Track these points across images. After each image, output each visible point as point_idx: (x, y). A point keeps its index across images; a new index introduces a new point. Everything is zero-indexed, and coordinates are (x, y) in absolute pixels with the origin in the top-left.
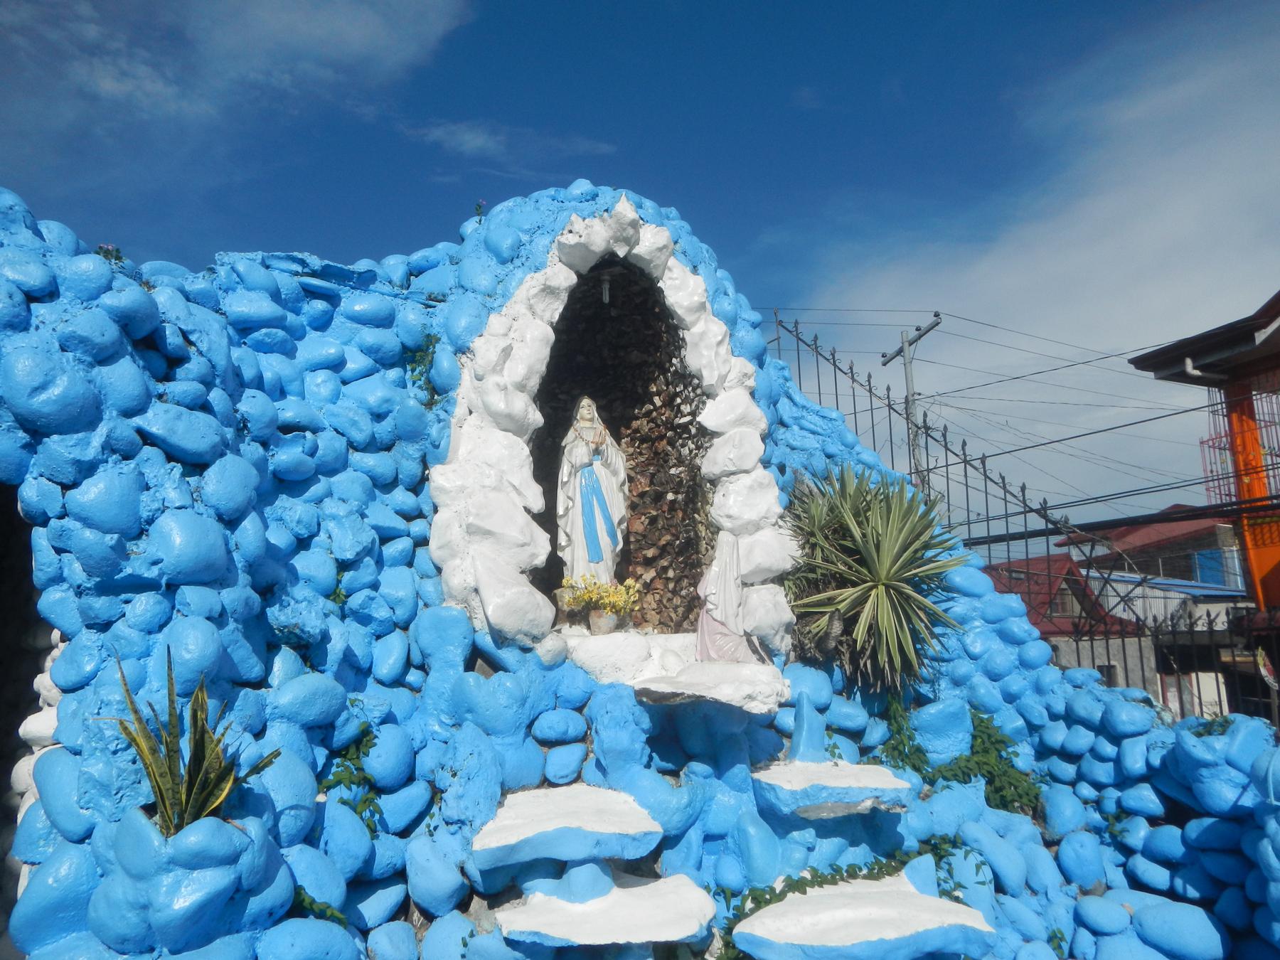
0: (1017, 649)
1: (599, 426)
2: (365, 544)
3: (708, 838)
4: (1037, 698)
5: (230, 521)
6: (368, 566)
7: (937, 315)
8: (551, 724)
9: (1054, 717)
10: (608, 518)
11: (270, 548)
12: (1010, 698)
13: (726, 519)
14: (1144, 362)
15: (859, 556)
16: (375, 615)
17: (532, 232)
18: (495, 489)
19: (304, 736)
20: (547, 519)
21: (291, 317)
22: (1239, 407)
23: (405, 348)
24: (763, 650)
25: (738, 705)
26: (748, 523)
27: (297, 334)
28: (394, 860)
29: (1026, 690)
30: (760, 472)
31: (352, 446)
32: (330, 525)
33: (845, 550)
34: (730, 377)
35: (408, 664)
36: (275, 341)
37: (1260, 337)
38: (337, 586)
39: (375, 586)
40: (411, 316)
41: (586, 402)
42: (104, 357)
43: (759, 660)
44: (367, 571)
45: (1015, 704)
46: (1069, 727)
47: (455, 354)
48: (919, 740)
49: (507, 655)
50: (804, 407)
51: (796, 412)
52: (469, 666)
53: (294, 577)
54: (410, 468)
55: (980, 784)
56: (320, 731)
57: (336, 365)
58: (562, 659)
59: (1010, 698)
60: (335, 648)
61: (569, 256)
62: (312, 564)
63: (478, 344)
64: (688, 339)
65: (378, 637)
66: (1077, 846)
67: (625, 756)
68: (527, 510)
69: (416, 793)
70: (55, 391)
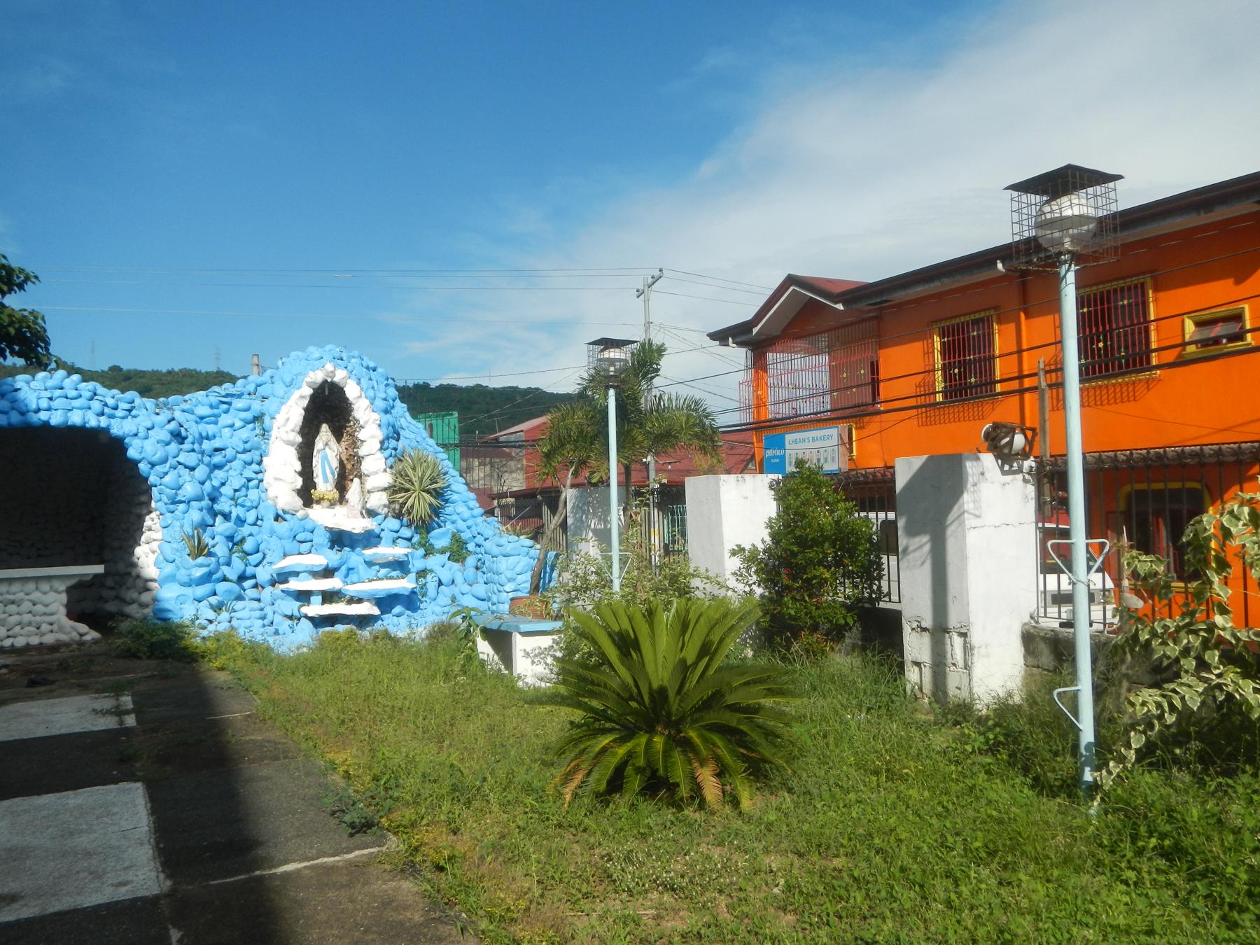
1: (330, 433)
3: (350, 569)
5: (203, 483)
7: (661, 270)
8: (301, 537)
10: (330, 467)
11: (213, 486)
12: (469, 528)
17: (297, 375)
20: (307, 473)
21: (215, 411)
22: (759, 364)
24: (371, 513)
30: (379, 455)
35: (257, 519)
37: (755, 330)
39: (246, 496)
40: (257, 406)
42: (168, 444)
44: (244, 491)
48: (432, 541)
49: (287, 516)
52: (276, 519)
53: (221, 494)
54: (257, 458)
55: (448, 554)
56: (230, 538)
57: (232, 426)
58: (306, 517)
59: (469, 528)
60: (234, 516)
61: (309, 385)
63: (278, 416)
67: (322, 545)
69: (258, 556)
70: (157, 456)
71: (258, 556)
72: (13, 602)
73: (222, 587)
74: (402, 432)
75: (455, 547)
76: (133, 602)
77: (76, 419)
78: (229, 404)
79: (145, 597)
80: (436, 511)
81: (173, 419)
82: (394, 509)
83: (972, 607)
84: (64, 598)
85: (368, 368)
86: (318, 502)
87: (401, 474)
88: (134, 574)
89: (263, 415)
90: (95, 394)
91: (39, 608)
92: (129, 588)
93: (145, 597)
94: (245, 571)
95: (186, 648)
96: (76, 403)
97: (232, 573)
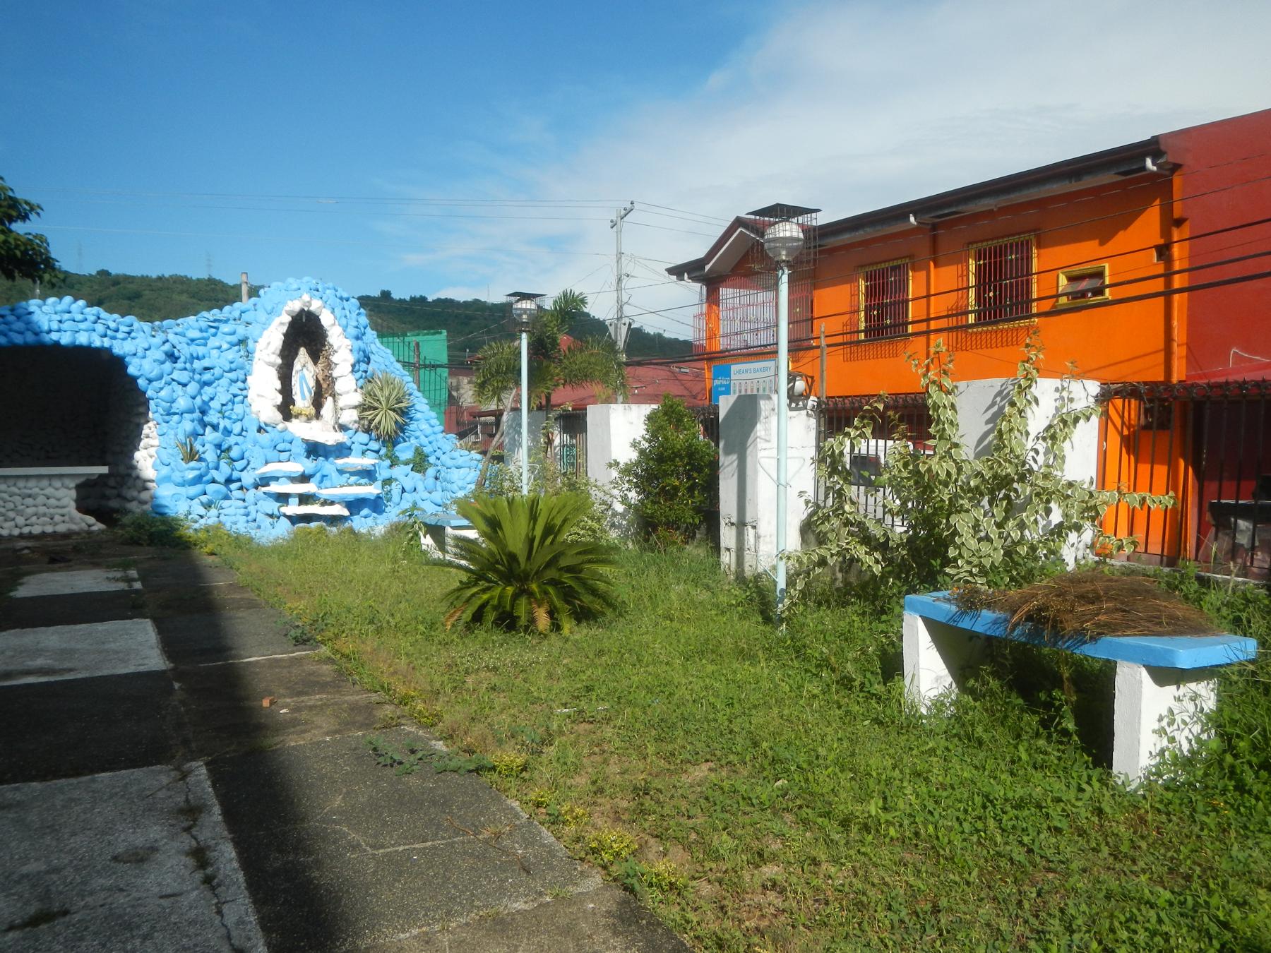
1: (307, 356)
3: (324, 476)
5: (194, 398)
7: (632, 203)
8: (280, 447)
10: (308, 387)
11: (203, 401)
12: (430, 443)
14: (671, 271)
20: (286, 390)
22: (712, 298)
24: (343, 428)
27: (208, 339)
35: (242, 430)
37: (707, 268)
40: (241, 331)
42: (163, 363)
48: (397, 454)
49: (268, 429)
53: (210, 408)
55: (411, 465)
56: (218, 446)
57: (219, 348)
58: (285, 430)
60: (221, 427)
61: (288, 313)
62: (215, 405)
63: (260, 340)
67: (299, 454)
69: (244, 462)
70: (154, 373)
71: (244, 462)
72: (30, 496)
73: (211, 488)
74: (372, 357)
75: (418, 459)
76: (133, 499)
77: (82, 339)
78: (217, 328)
79: (144, 496)
80: (401, 428)
81: (167, 341)
82: (363, 425)
83: (760, 507)
84: (73, 493)
85: (341, 299)
86: (297, 417)
87: (370, 394)
88: (134, 475)
89: (247, 338)
90: (99, 318)
91: (52, 502)
92: (129, 488)
93: (144, 496)
94: (231, 475)
95: (180, 537)
96: (82, 326)
97: (220, 477)
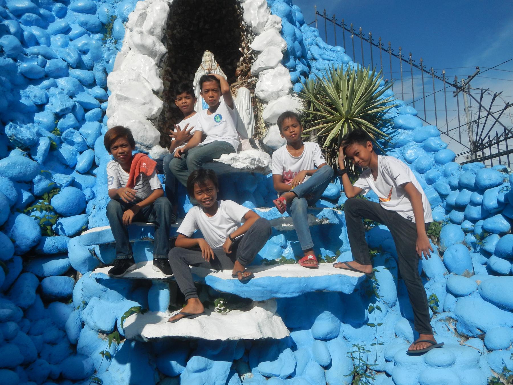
0: (434, 155)
2: (67, 106)
4: (445, 179)
6: (70, 117)
9: (453, 188)
13: (261, 93)
15: (333, 106)
16: (75, 140)
18: (134, 80)
19: (11, 184)
23: (103, 24)
25: (227, 163)
26: (272, 93)
28: (56, 245)
29: (439, 177)
30: (281, 68)
31: (69, 66)
32: (52, 99)
33: (329, 104)
34: (267, 24)
36: (33, 19)
38: (56, 127)
41: (207, 53)
43: (253, 147)
45: (433, 185)
46: (460, 191)
47: (123, 23)
50: (324, 48)
51: (321, 51)
57: (66, 31)
59: (430, 182)
64: (244, 8)
65: (81, 153)
66: (453, 251)
68: (154, 91)
74: (313, 64)
89: (113, 18)
